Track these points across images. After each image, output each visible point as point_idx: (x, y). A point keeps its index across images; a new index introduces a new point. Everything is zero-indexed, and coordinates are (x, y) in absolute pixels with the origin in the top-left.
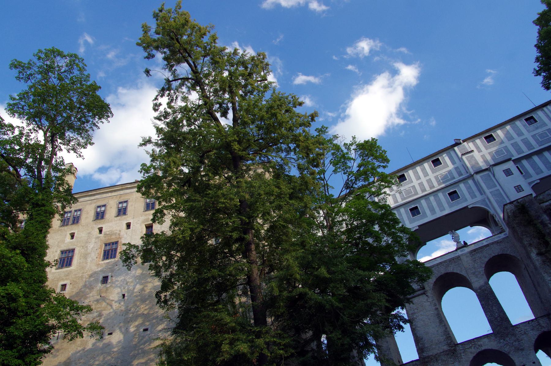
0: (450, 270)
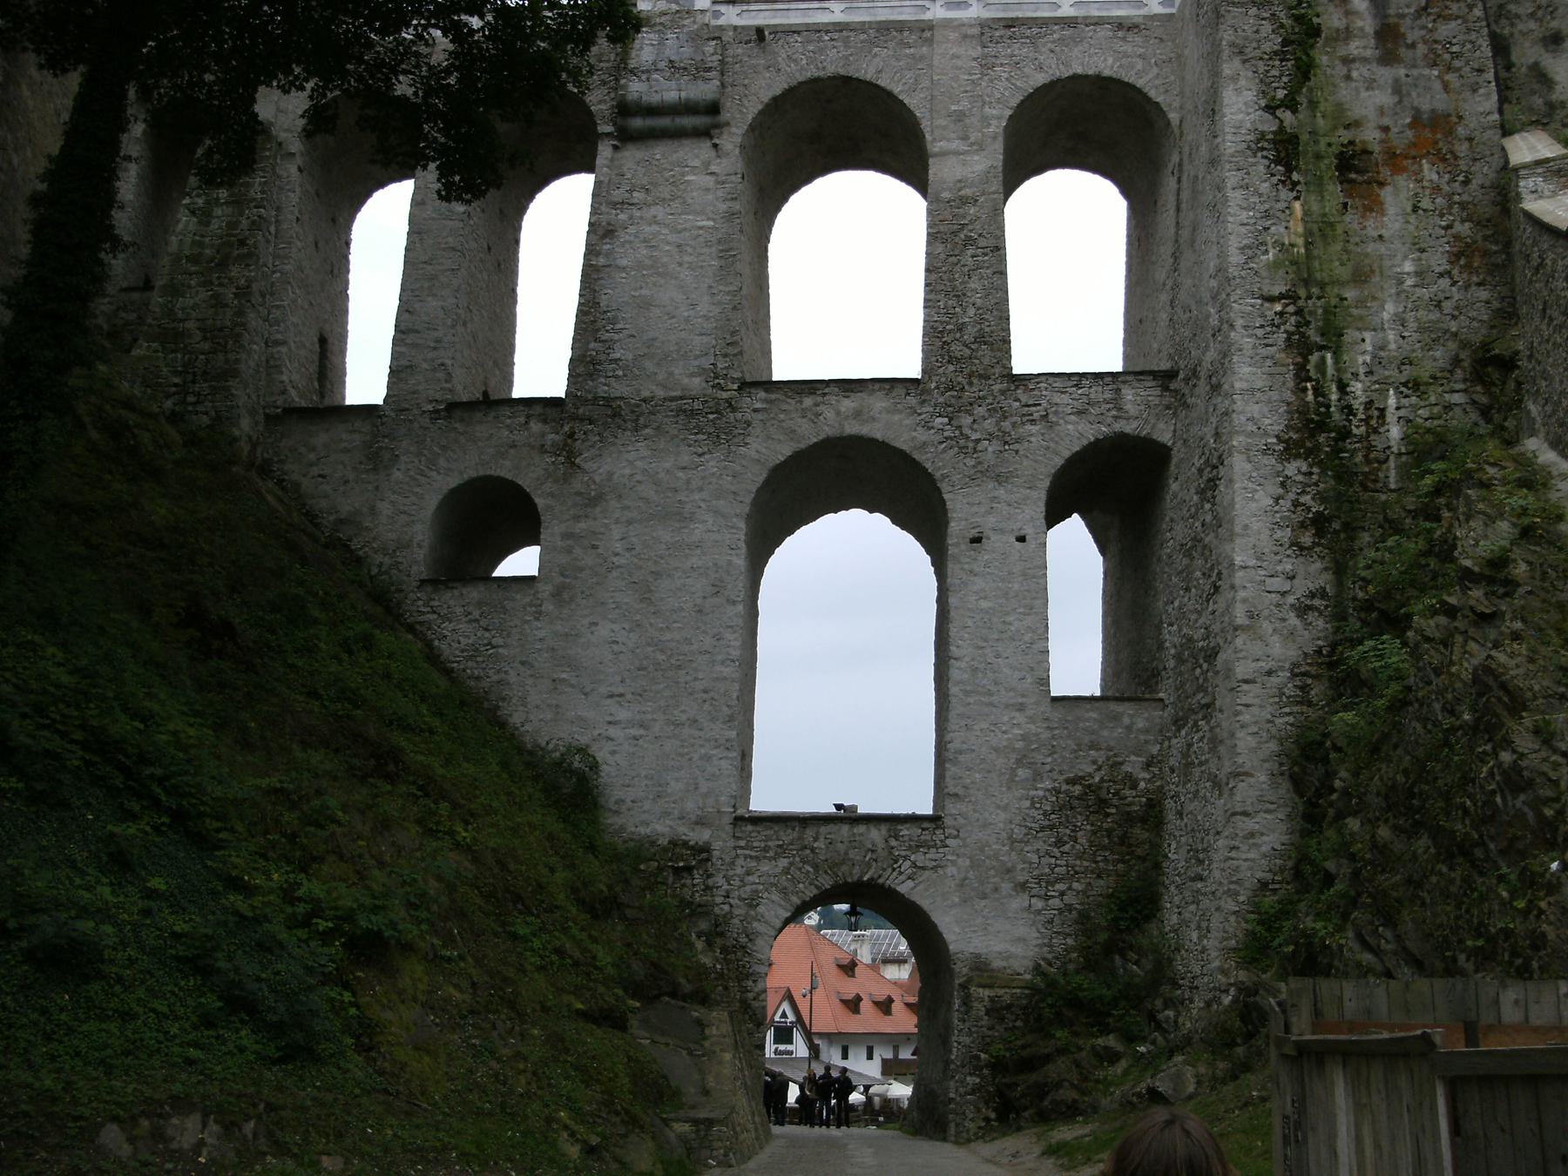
0: (866, 70)
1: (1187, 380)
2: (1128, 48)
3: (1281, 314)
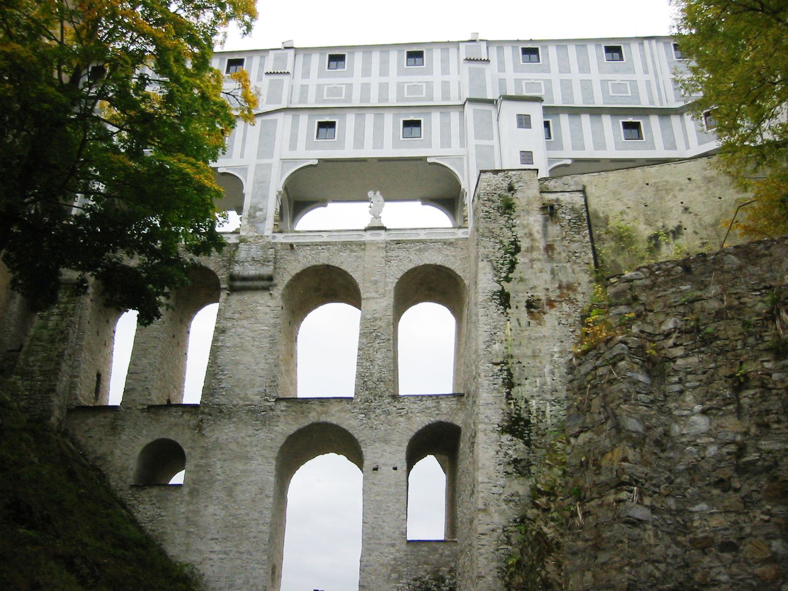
0: (335, 262)
1: (467, 397)
2: (448, 253)
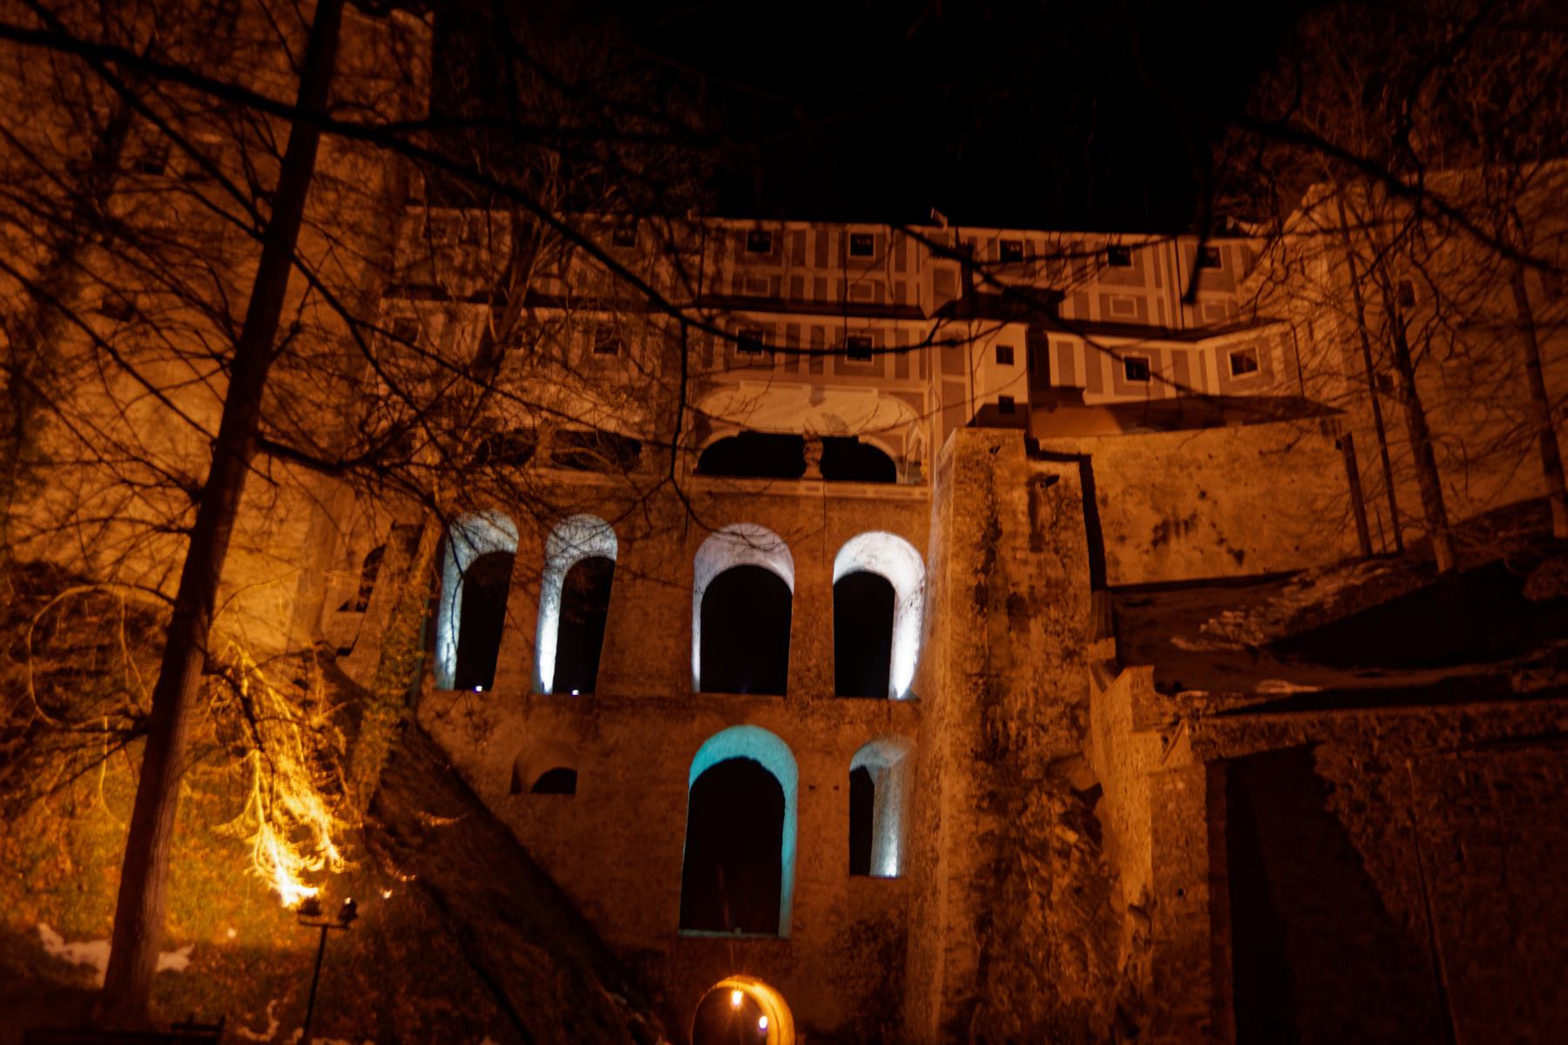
3: (976, 684)
